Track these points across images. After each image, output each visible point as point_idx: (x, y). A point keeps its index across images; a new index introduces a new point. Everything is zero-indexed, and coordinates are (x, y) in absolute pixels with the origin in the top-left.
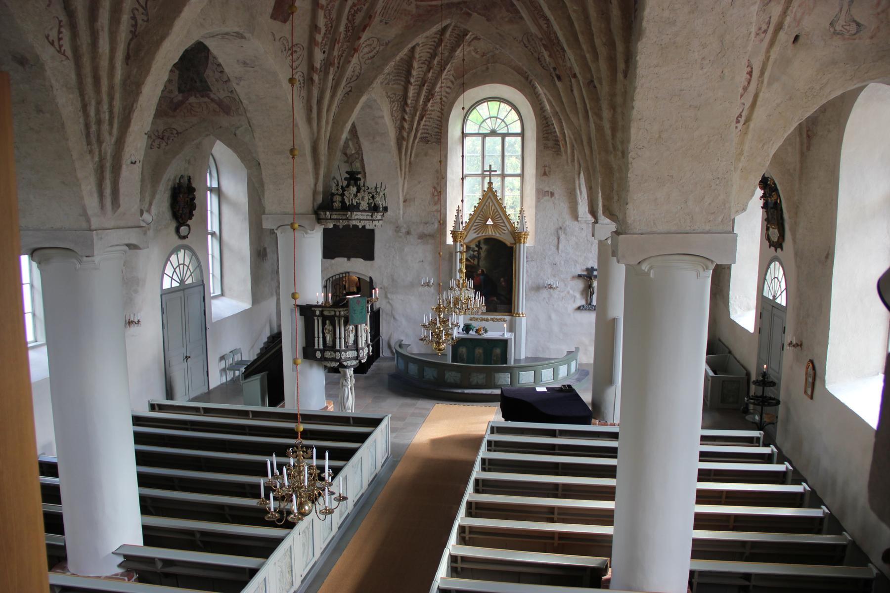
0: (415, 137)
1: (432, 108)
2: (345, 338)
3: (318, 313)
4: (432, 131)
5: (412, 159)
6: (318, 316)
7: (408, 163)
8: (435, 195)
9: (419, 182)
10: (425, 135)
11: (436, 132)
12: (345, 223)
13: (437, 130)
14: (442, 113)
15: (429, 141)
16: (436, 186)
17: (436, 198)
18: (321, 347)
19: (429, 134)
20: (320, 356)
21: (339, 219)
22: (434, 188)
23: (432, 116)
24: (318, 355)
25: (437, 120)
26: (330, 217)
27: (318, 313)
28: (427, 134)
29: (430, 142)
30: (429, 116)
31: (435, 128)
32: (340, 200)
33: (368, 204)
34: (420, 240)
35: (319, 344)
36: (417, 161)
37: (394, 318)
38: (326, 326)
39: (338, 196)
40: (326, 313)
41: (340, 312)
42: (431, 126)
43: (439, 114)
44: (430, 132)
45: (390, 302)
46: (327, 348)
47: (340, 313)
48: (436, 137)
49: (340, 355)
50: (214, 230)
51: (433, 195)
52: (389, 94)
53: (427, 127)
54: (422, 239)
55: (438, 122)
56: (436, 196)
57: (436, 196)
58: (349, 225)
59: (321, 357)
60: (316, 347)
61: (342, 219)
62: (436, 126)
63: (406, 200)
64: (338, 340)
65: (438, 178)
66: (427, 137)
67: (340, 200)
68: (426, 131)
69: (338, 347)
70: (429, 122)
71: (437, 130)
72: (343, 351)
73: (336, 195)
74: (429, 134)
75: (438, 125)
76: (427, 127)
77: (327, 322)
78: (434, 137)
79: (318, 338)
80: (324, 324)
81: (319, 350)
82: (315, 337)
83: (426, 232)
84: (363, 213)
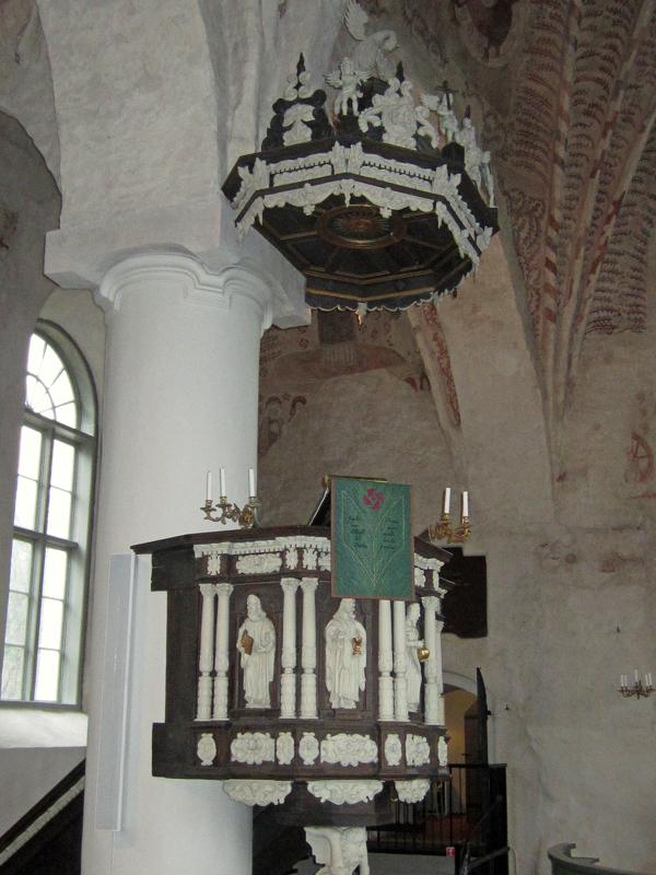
0: (578, 317)
1: (617, 247)
2: (320, 671)
3: (214, 567)
4: (621, 304)
5: (574, 372)
6: (214, 580)
7: (562, 378)
8: (639, 455)
9: (597, 427)
10: (603, 314)
11: (630, 306)
12: (321, 194)
13: (631, 300)
14: (641, 261)
15: (614, 328)
16: (640, 432)
17: (644, 463)
18: (221, 714)
19: (612, 310)
20: (213, 752)
21: (301, 185)
22: (636, 437)
23: (617, 267)
24: (207, 749)
25: (632, 277)
26: (271, 183)
27: (214, 567)
28: (608, 311)
29: (616, 330)
30: (609, 267)
31: (628, 295)
32: (310, 118)
33: (416, 136)
34: (607, 575)
35: (212, 703)
36: (588, 376)
37: (547, 796)
38: (247, 625)
39: (300, 107)
40: (245, 567)
41: (300, 551)
42: (616, 292)
43: (634, 262)
44: (615, 307)
45: (535, 746)
46: (244, 721)
47: (301, 558)
48: (632, 316)
49: (297, 745)
50: (76, 540)
51: (635, 456)
52: (506, 187)
53: (608, 295)
54: (613, 571)
55: (633, 282)
56: (642, 457)
57: (642, 457)
58: (342, 196)
59: (216, 761)
60: (203, 715)
61: (314, 182)
62: (630, 291)
63: (565, 474)
64: (288, 681)
65: (644, 413)
66: (609, 320)
67: (310, 118)
68: (605, 304)
69: (288, 711)
70: (612, 281)
71: (631, 300)
72: (309, 725)
73: (291, 104)
74: (612, 310)
75: (633, 288)
76: (608, 295)
77: (253, 602)
78: (625, 316)
79: (213, 674)
80: (238, 617)
81: (210, 727)
82: (201, 674)
83: (625, 553)
84: (392, 163)
